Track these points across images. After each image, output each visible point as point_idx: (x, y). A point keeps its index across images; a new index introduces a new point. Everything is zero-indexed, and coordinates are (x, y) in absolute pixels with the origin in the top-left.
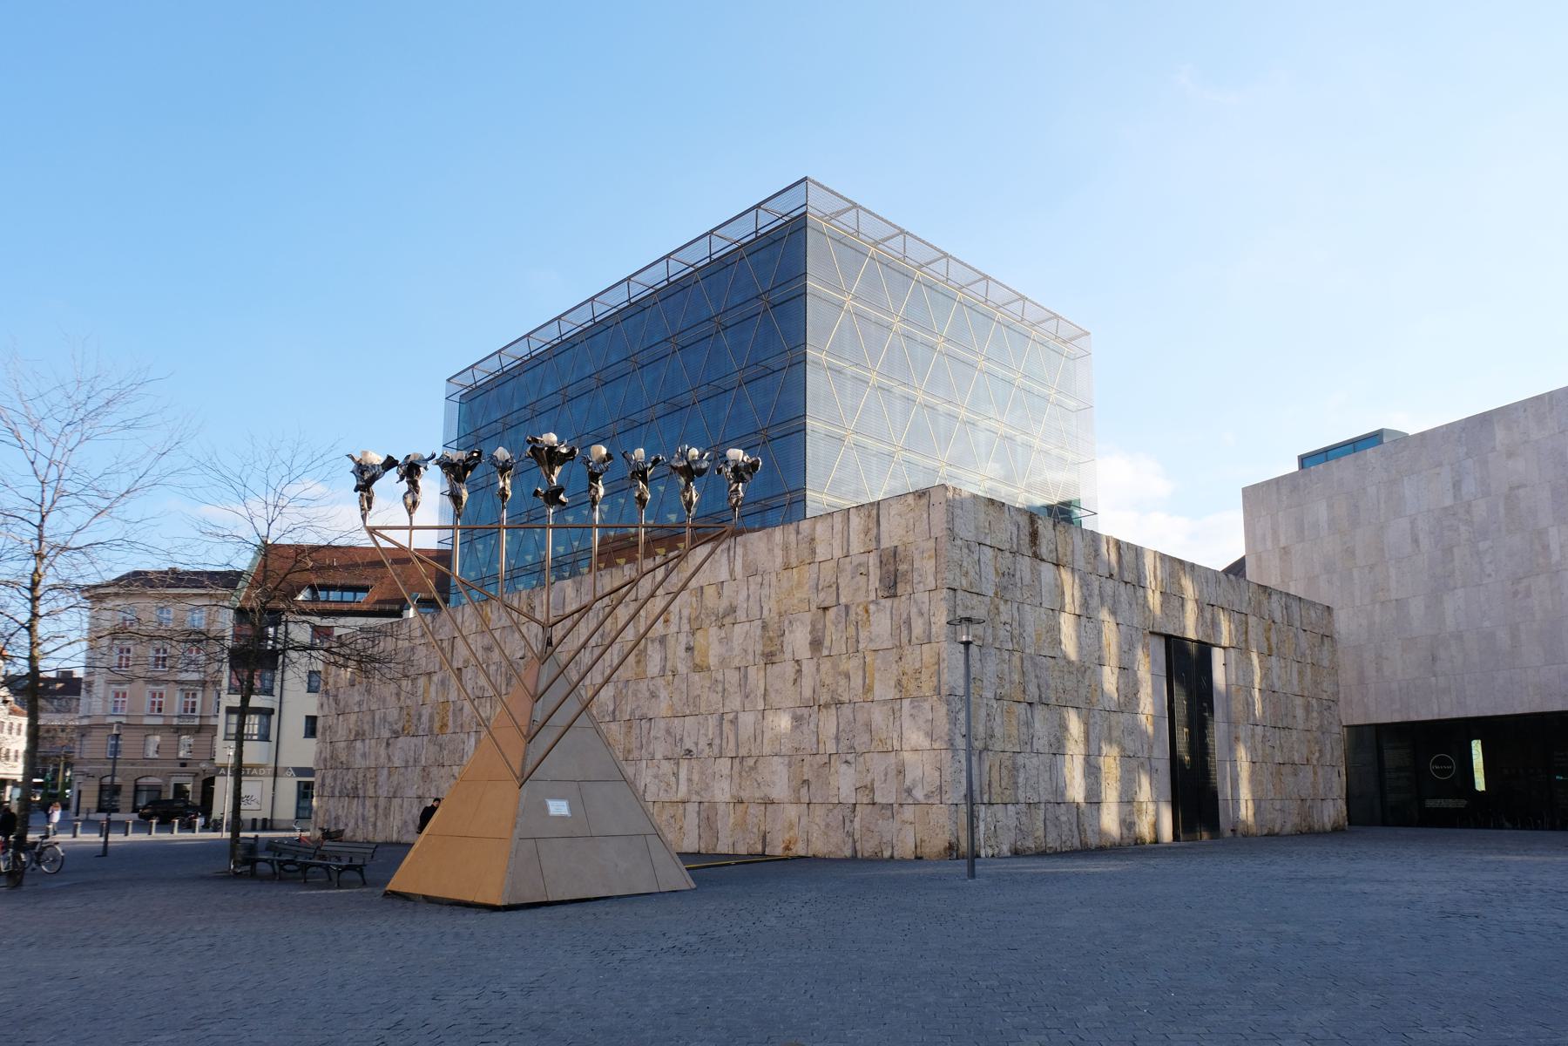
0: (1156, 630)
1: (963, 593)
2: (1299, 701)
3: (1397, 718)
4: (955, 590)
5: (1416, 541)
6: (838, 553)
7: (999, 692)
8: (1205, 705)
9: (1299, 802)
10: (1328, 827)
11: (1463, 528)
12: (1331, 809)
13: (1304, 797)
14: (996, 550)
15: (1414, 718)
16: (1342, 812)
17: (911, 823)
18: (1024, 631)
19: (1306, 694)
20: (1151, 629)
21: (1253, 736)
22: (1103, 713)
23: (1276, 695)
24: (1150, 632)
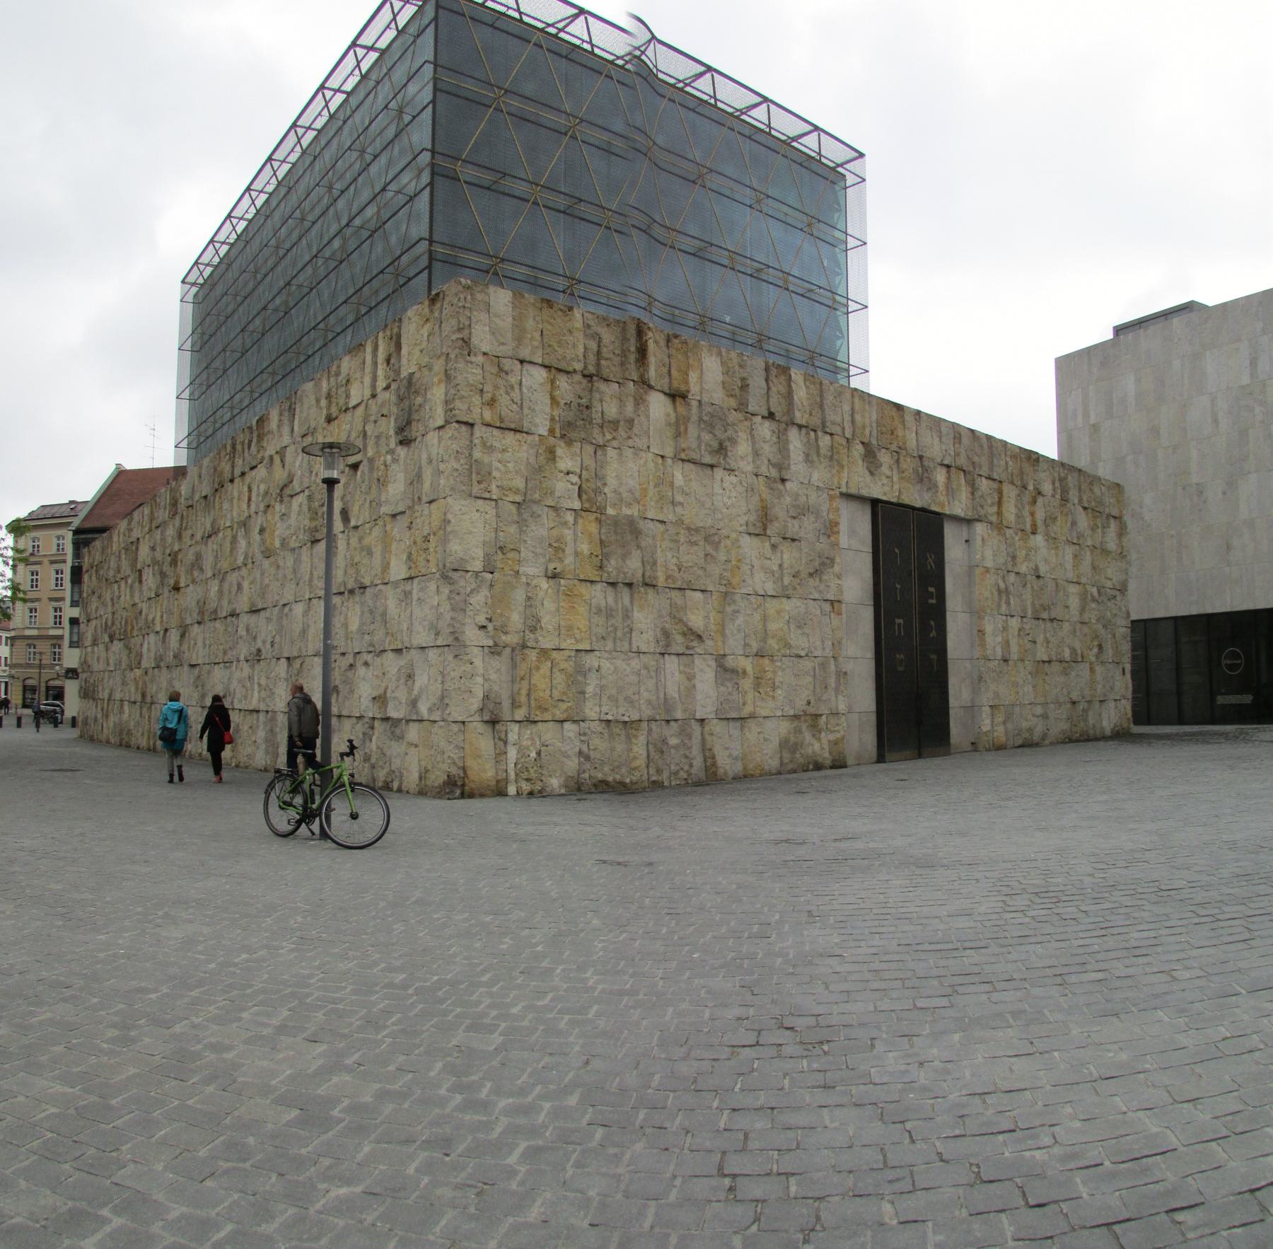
0: (853, 491)
1: (484, 428)
2: (1073, 589)
3: (1194, 611)
4: (472, 425)
5: (1216, 421)
6: (368, 393)
7: (551, 566)
8: (931, 589)
9: (1069, 706)
10: (1108, 732)
11: (1258, 410)
12: (1112, 712)
13: (1075, 696)
14: (553, 370)
15: (1209, 610)
16: (1126, 714)
17: (416, 746)
18: (605, 484)
19: (1084, 580)
20: (844, 490)
21: (1005, 629)
22: (753, 599)
23: (1041, 582)
24: (842, 494)
